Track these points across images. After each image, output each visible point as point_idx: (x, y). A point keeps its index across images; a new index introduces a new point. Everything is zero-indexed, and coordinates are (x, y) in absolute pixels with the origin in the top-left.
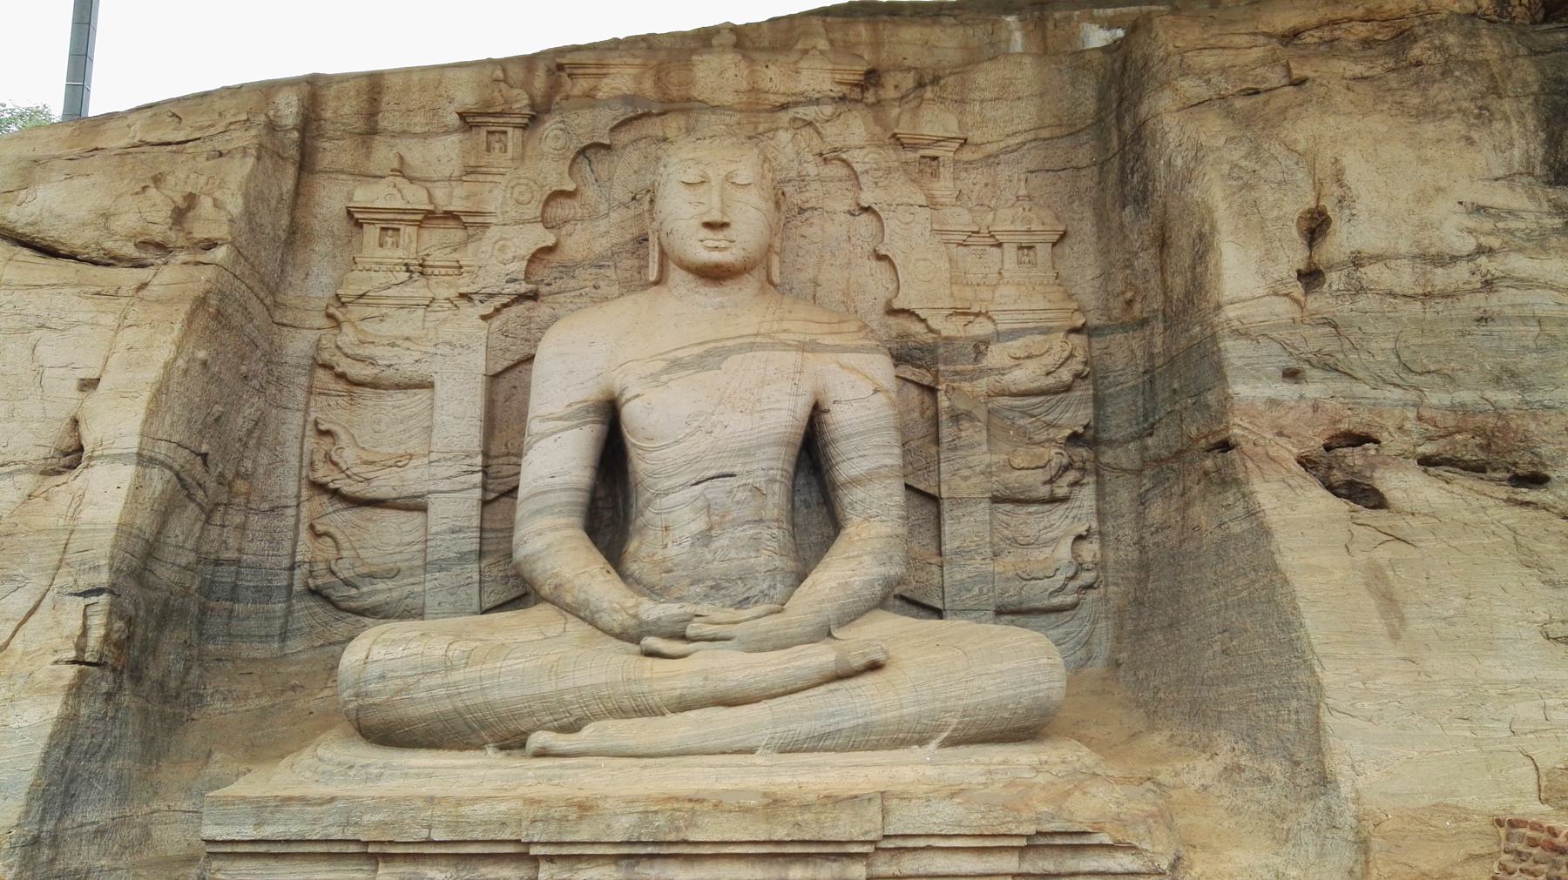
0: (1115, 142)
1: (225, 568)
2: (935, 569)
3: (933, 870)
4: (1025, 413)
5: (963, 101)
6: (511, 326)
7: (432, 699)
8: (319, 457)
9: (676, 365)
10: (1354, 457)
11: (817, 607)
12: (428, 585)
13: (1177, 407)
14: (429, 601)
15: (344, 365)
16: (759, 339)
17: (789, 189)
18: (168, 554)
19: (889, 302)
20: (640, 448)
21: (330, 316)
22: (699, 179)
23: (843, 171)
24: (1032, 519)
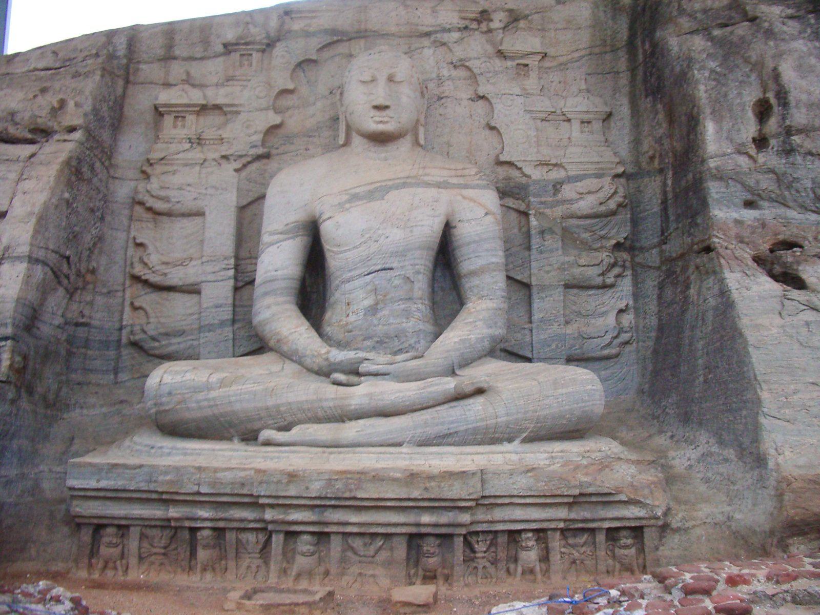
0: (641, 57)
2: (527, 332)
3: (513, 517)
4: (586, 230)
5: (543, 30)
7: (200, 408)
9: (355, 198)
10: (788, 256)
12: (202, 341)
13: (680, 225)
15: (150, 202)
16: (409, 180)
17: (431, 85)
18: (46, 317)
19: (497, 156)
20: (333, 252)
22: (370, 79)
24: (590, 300)
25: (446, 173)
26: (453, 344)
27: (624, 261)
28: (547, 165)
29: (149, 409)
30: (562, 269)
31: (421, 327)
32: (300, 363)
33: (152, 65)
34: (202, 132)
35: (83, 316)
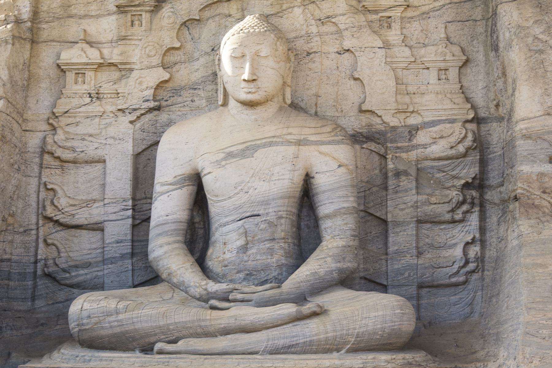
1: (5, 263)
2: (384, 262)
4: (440, 170)
6: (146, 126)
7: (111, 327)
8: (48, 203)
9: (230, 155)
11: (298, 285)
12: (106, 272)
14: (106, 280)
15: (59, 152)
16: (275, 140)
21: (49, 124)
22: (241, 55)
23: (333, 29)
24: (442, 234)
25: (307, 131)
26: (304, 276)
27: (473, 198)
28: (405, 112)
29: (73, 328)
30: (416, 206)
31: (283, 262)
32: (187, 292)
33: (52, 24)
34: (100, 87)
35: (6, 253)
